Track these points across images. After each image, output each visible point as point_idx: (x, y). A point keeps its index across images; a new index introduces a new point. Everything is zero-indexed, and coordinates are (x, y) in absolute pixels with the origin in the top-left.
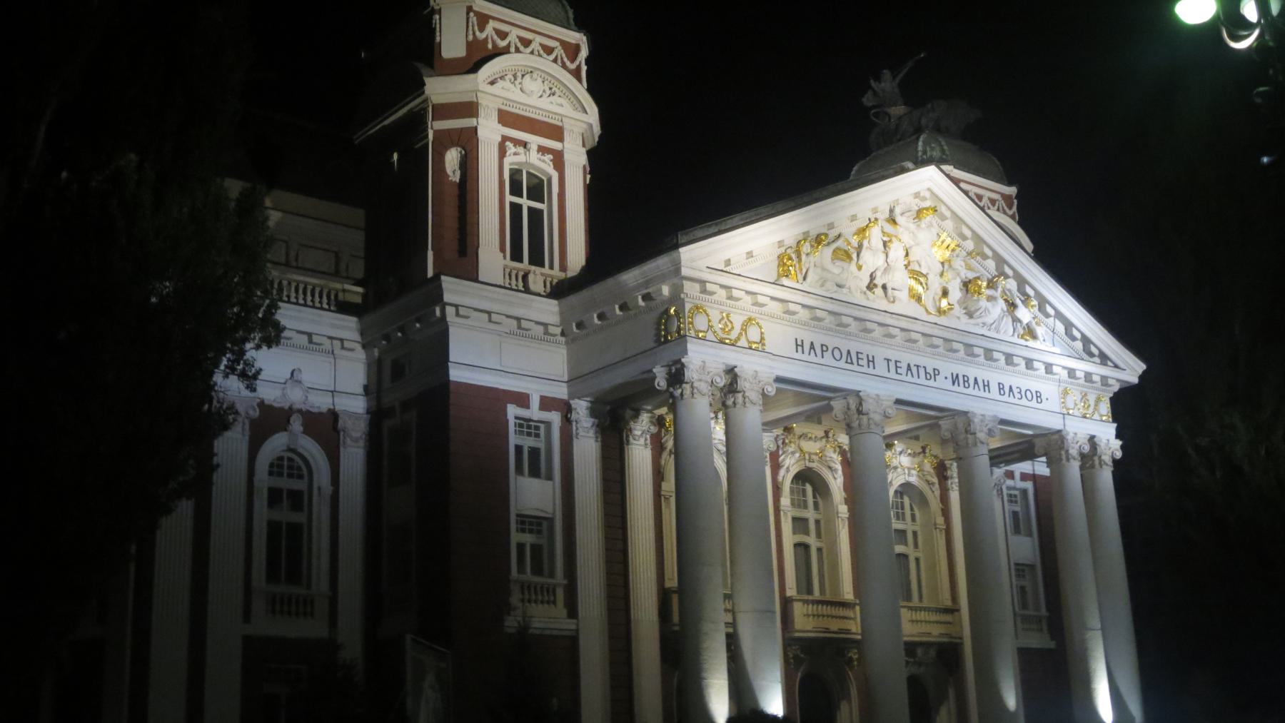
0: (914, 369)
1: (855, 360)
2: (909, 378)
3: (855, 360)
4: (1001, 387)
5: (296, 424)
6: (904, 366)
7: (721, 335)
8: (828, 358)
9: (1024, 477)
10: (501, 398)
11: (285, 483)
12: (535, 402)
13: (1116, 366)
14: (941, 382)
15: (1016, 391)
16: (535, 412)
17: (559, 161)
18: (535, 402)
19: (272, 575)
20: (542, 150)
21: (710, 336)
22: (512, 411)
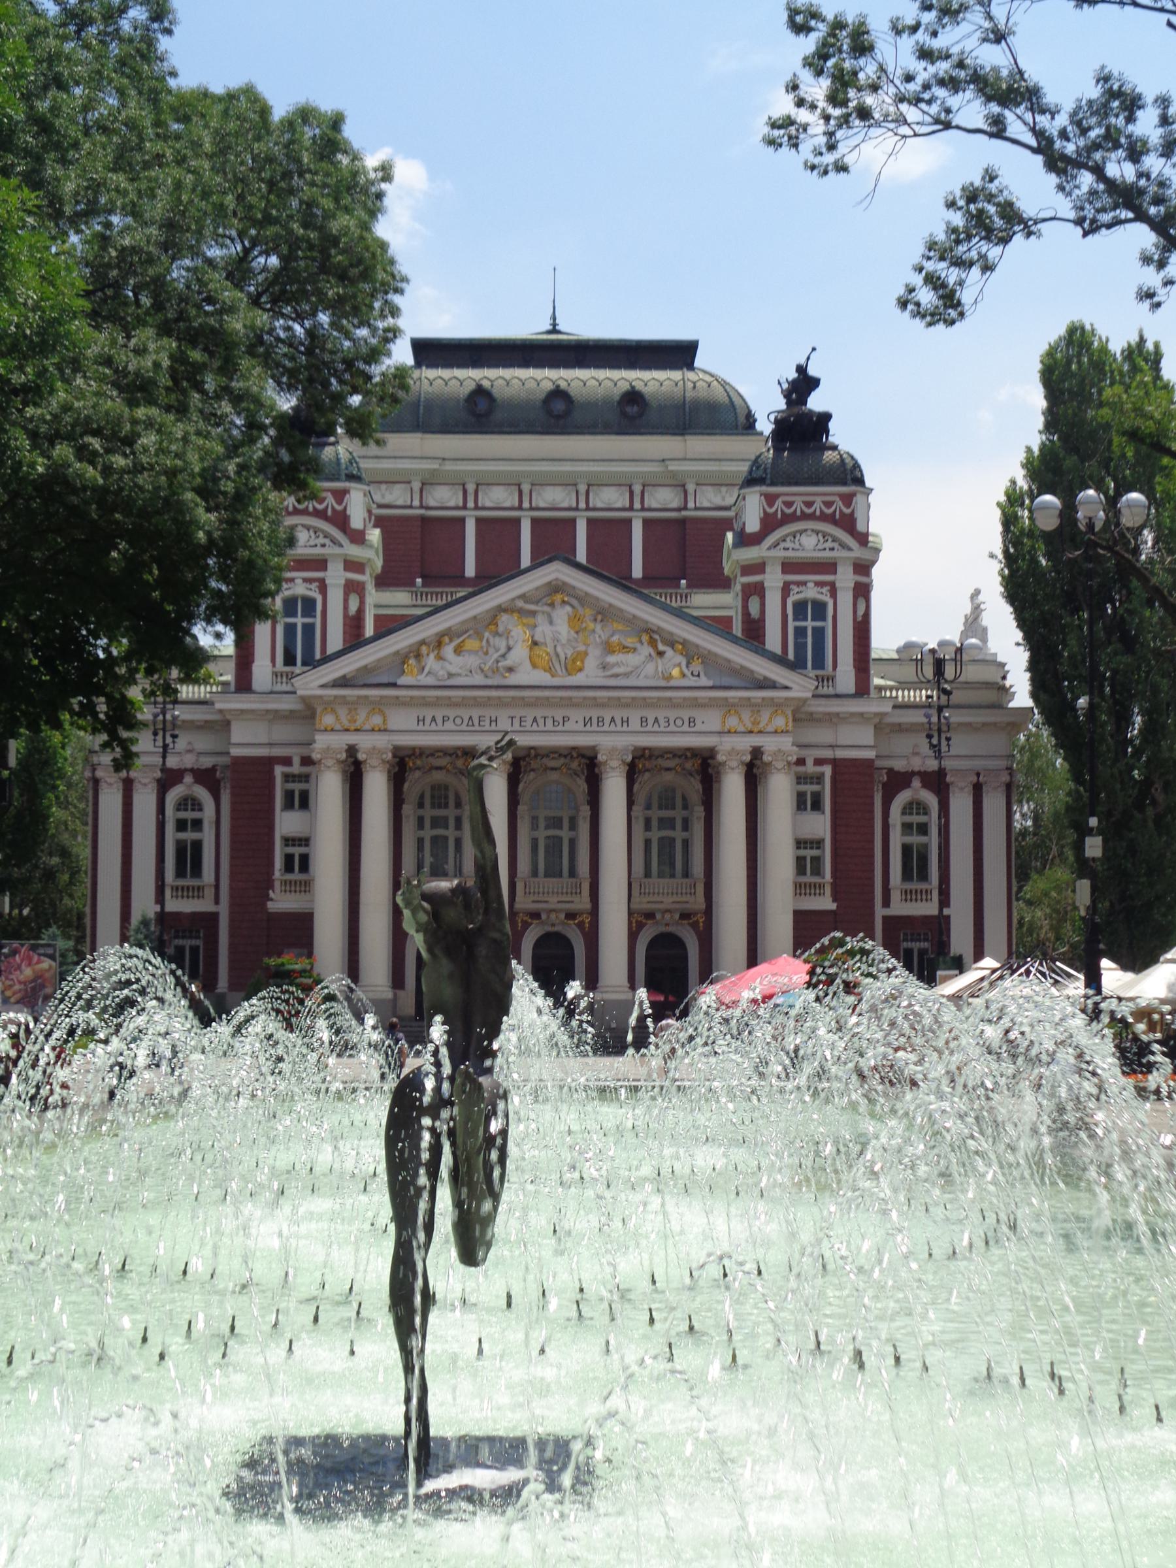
0: (541, 722)
1: (476, 721)
2: (535, 727)
3: (476, 721)
4: (644, 721)
5: (188, 779)
6: (530, 720)
7: (346, 724)
8: (449, 725)
9: (819, 762)
10: (271, 761)
11: (189, 815)
12: (296, 761)
13: (786, 688)
14: (569, 726)
15: (661, 721)
16: (296, 768)
17: (323, 588)
18: (296, 761)
19: (180, 873)
20: (305, 580)
21: (338, 727)
22: (279, 770)
